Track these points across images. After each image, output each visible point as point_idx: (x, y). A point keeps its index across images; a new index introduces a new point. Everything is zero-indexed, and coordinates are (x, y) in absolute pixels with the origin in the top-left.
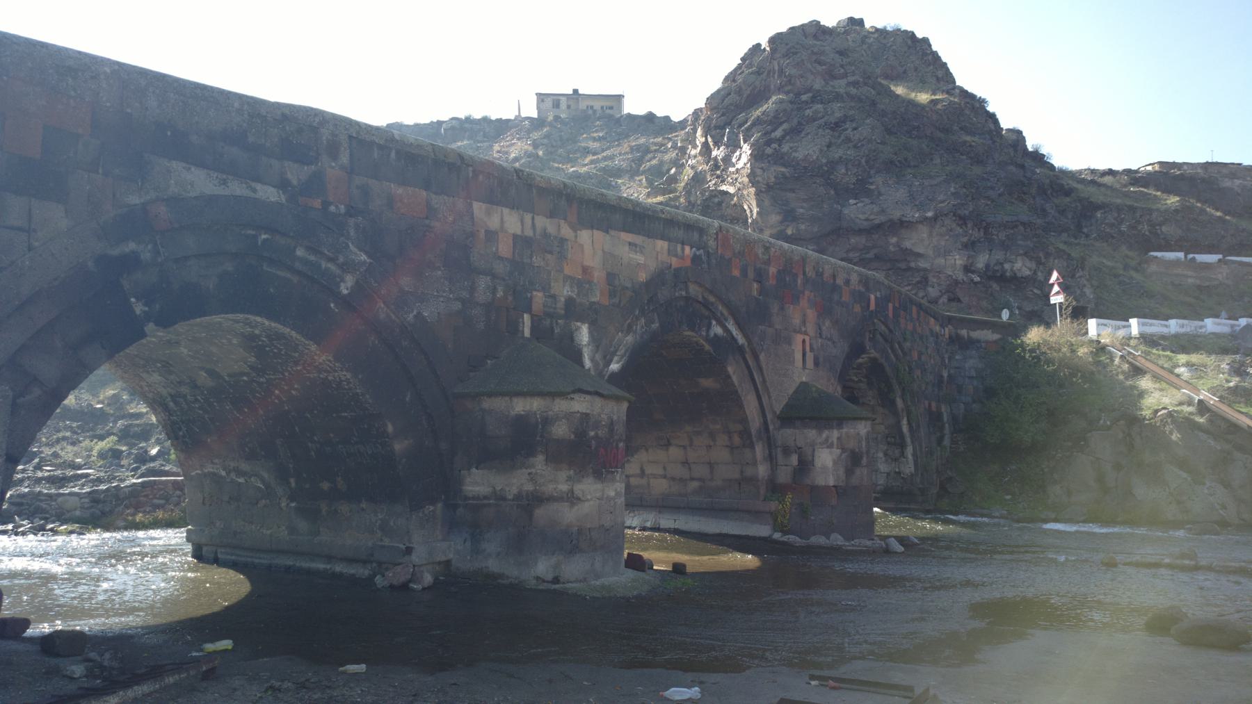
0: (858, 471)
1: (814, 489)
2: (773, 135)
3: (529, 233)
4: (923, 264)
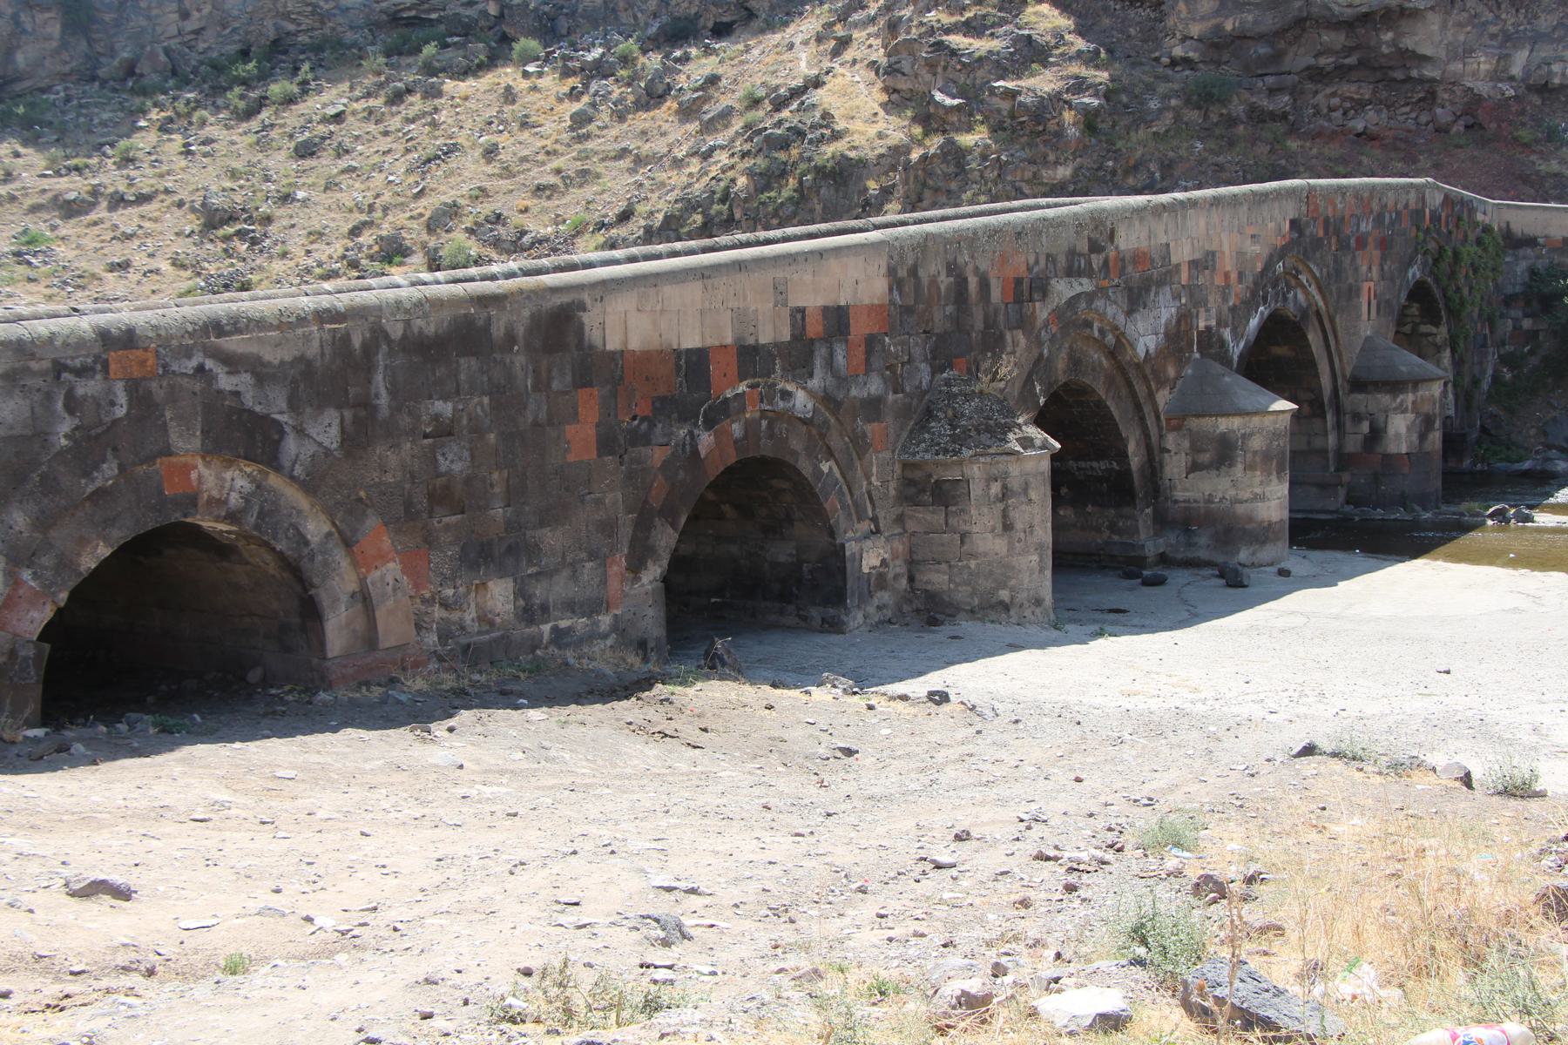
1: (1387, 457)
4: (1429, 72)
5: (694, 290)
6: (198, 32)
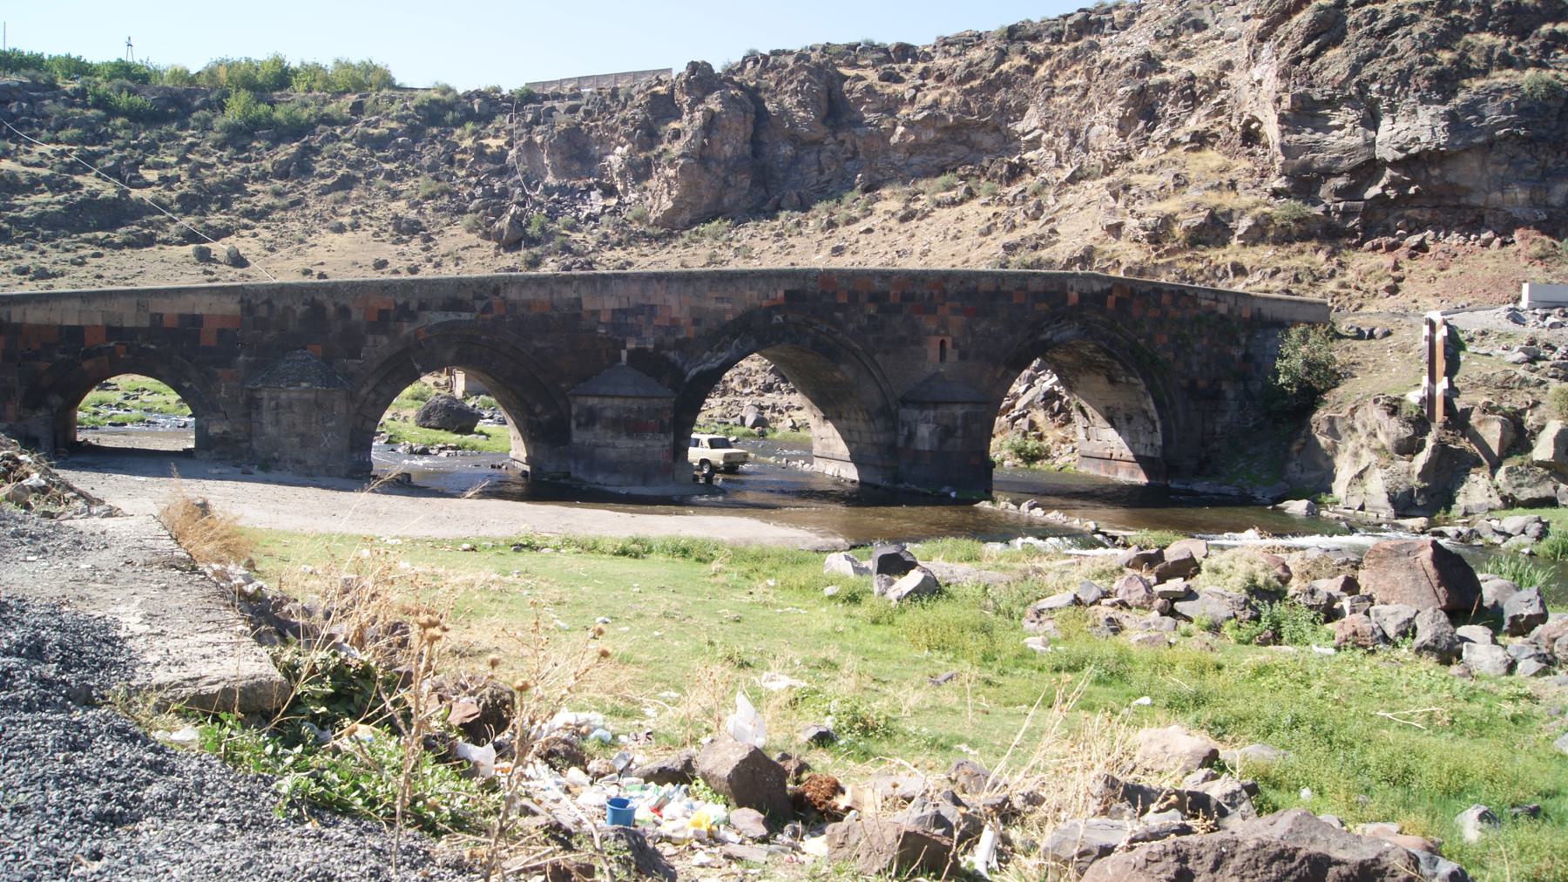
0: (950, 441)
1: (917, 452)
2: (1304, 51)
3: (625, 305)
4: (1477, 200)
5: (77, 304)
6: (828, 182)
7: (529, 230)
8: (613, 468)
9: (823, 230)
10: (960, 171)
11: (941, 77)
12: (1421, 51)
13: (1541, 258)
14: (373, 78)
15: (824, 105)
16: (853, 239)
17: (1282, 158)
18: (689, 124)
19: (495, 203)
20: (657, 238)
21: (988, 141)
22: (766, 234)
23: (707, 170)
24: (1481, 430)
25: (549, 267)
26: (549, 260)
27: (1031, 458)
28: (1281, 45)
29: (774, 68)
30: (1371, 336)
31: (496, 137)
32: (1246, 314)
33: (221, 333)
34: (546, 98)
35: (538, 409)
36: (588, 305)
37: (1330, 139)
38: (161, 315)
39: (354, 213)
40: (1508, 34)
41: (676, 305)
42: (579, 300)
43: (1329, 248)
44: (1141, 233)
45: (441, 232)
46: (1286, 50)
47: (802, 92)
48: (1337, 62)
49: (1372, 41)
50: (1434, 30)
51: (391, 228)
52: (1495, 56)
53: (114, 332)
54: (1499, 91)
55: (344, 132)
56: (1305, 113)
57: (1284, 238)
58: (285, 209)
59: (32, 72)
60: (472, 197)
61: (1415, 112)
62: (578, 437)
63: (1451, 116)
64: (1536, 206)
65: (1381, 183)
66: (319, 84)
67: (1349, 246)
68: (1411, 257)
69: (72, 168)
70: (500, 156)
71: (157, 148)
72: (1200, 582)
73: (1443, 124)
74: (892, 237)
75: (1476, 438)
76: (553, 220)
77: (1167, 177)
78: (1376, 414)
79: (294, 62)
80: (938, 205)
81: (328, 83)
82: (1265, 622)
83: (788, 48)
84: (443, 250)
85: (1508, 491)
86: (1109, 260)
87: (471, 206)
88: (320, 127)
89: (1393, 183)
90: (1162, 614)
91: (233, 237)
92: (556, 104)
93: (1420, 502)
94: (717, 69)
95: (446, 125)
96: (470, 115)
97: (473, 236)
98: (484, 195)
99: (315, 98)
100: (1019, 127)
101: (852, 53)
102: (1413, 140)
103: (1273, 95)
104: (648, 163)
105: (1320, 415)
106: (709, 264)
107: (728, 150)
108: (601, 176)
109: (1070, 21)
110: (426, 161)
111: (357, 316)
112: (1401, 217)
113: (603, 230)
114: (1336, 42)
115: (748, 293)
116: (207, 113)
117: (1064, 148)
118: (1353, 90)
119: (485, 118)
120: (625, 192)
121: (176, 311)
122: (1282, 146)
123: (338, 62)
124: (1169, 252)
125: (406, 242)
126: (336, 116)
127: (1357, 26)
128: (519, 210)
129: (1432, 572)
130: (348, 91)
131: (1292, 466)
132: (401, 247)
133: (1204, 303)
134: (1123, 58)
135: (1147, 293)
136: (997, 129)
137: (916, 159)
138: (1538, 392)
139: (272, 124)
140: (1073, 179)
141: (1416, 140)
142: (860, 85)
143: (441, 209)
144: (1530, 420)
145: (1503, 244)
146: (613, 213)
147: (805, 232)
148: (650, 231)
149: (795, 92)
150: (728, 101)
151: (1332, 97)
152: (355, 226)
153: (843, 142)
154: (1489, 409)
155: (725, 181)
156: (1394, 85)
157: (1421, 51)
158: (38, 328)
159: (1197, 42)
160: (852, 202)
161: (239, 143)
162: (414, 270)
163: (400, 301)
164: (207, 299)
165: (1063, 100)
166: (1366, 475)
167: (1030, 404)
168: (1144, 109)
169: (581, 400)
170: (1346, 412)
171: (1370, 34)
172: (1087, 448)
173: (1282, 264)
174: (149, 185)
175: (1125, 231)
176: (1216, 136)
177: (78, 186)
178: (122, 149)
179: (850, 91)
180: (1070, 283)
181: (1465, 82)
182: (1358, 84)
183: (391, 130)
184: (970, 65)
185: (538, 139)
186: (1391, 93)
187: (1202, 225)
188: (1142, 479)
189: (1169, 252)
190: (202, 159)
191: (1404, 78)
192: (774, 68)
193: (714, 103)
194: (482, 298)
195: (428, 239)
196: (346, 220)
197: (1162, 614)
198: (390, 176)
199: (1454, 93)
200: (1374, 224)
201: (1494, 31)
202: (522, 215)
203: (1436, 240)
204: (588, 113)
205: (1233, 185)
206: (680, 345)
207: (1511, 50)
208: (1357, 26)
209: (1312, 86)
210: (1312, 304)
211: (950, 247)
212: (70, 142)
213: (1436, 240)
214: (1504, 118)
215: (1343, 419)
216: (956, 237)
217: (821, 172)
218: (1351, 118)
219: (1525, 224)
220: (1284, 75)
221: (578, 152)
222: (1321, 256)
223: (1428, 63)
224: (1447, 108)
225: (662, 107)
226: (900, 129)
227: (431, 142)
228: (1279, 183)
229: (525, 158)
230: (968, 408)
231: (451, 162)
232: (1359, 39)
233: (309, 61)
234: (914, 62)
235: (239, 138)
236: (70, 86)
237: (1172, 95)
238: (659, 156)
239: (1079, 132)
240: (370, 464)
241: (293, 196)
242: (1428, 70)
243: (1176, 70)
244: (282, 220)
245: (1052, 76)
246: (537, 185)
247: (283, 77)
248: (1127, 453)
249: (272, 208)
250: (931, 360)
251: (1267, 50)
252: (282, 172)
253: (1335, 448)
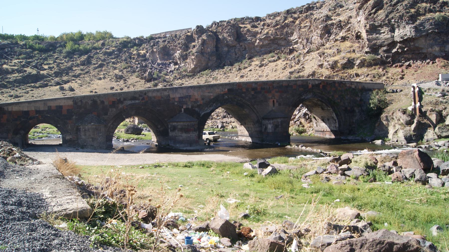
2: (372, 12)
3: (182, 96)
4: (425, 51)
5: (27, 104)
6: (238, 57)
7: (154, 76)
8: (181, 142)
9: (237, 71)
10: (276, 52)
11: (268, 26)
12: (406, 9)
13: (444, 66)
14: (107, 36)
15: (236, 35)
16: (246, 73)
17: (367, 43)
18: (197, 43)
19: (144, 69)
20: (190, 76)
21: (283, 43)
22: (221, 73)
23: (203, 56)
24: (430, 117)
25: (160, 86)
26: (160, 84)
27: (301, 132)
28: (365, 10)
29: (221, 26)
30: (397, 92)
31: (143, 50)
32: (360, 88)
33: (68, 110)
34: (156, 38)
35: (159, 127)
36: (171, 96)
37: (381, 36)
38: (51, 106)
39: (104, 74)
40: (430, 3)
41: (197, 95)
42: (169, 95)
43: (383, 67)
44: (329, 66)
45: (129, 78)
46: (367, 12)
47: (229, 32)
48: (381, 14)
49: (391, 8)
50: (409, 3)
51: (114, 78)
52: (427, 10)
53: (38, 112)
54: (429, 19)
55: (100, 51)
56: (373, 29)
57: (370, 65)
58: (84, 74)
59: (11, 40)
60: (137, 68)
61: (405, 27)
62: (171, 134)
63: (416, 28)
64: (442, 52)
65: (397, 48)
66: (92, 38)
67: (388, 67)
68: (407, 68)
69: (23, 66)
70: (144, 55)
71: (47, 59)
72: (352, 165)
73: (413, 30)
74: (257, 72)
75: (429, 119)
76: (160, 73)
77: (334, 50)
78: (399, 114)
79: (84, 32)
80: (270, 62)
81: (94, 38)
82: (371, 176)
83: (224, 20)
84: (130, 83)
85: (439, 134)
86: (320, 74)
87: (137, 70)
88: (93, 50)
89: (400, 48)
90: (341, 175)
91: (70, 83)
92: (159, 40)
93: (414, 139)
94: (205, 27)
95: (129, 48)
96: (135, 45)
97: (138, 79)
98: (140, 67)
99: (91, 42)
100: (292, 38)
101: (243, 20)
102: (405, 35)
103: (364, 25)
104: (186, 55)
105: (383, 115)
106: (205, 83)
107: (209, 50)
108: (173, 59)
109: (304, 7)
110: (123, 58)
111: (106, 103)
112: (403, 57)
113: (175, 75)
114: (381, 9)
115: (217, 90)
116: (61, 48)
117: (305, 44)
118: (387, 22)
119: (139, 45)
120: (181, 63)
121: (55, 105)
122: (367, 39)
123: (97, 32)
124: (337, 71)
125: (119, 81)
126: (97, 47)
127: (387, 3)
128: (151, 70)
129: (419, 158)
130: (100, 40)
131: (376, 130)
132: (118, 83)
133: (348, 85)
134: (320, 17)
135: (331, 83)
136: (285, 39)
137: (263, 49)
138: (446, 105)
139: (79, 50)
140: (308, 52)
141: (406, 35)
142: (246, 29)
143: (129, 72)
144: (444, 113)
145: (433, 63)
146: (177, 70)
147: (232, 72)
148: (188, 74)
149: (227, 32)
150: (208, 36)
151: (381, 24)
152: (104, 78)
153: (242, 46)
154: (432, 111)
155: (209, 58)
156: (398, 20)
157: (406, 9)
158: (16, 112)
159: (341, 11)
160: (245, 63)
161: (70, 56)
162: (122, 89)
163: (118, 98)
164: (63, 101)
165: (304, 30)
166: (398, 131)
167: (300, 117)
168: (327, 31)
169: (171, 123)
170: (391, 114)
171: (391, 5)
172: (317, 129)
173: (370, 73)
174: (45, 69)
175: (324, 66)
176: (348, 37)
177: (26, 71)
178: (37, 60)
179: (243, 31)
180: (309, 82)
181: (419, 17)
182: (388, 20)
183: (113, 50)
184: (277, 21)
185: (155, 50)
186: (398, 22)
187: (346, 63)
188: (333, 137)
189: (337, 71)
190: (60, 62)
191: (401, 17)
192: (221, 26)
193: (204, 37)
194: (141, 96)
195: (125, 80)
196: (102, 76)
197: (341, 175)
198: (114, 63)
199: (416, 21)
200: (395, 60)
201: (426, 2)
202: (152, 72)
203: (413, 63)
204: (169, 42)
205: (354, 51)
206: (199, 106)
207: (431, 7)
208: (387, 3)
209: (375, 21)
210: (379, 84)
211: (274, 74)
212: (23, 59)
213: (413, 63)
214: (431, 27)
215: (390, 116)
216: (275, 71)
217: (236, 55)
218: (387, 30)
219: (439, 57)
220: (367, 19)
221: (166, 53)
222: (381, 70)
223: (408, 13)
224: (414, 25)
225: (190, 39)
226: (258, 41)
227: (125, 53)
228: (367, 50)
229: (151, 56)
230: (282, 119)
231: (130, 58)
232: (387, 7)
233: (89, 32)
234: (261, 22)
235: (70, 55)
236: (22, 43)
237: (335, 26)
238: (190, 53)
239: (309, 39)
240: (112, 145)
241: (86, 70)
242: (408, 15)
243: (335, 19)
244: (84, 77)
245: (300, 23)
246: (155, 63)
247: (82, 37)
248: (328, 129)
249: (80, 74)
250: (271, 106)
251: (361, 12)
252: (83, 64)
253: (388, 124)
